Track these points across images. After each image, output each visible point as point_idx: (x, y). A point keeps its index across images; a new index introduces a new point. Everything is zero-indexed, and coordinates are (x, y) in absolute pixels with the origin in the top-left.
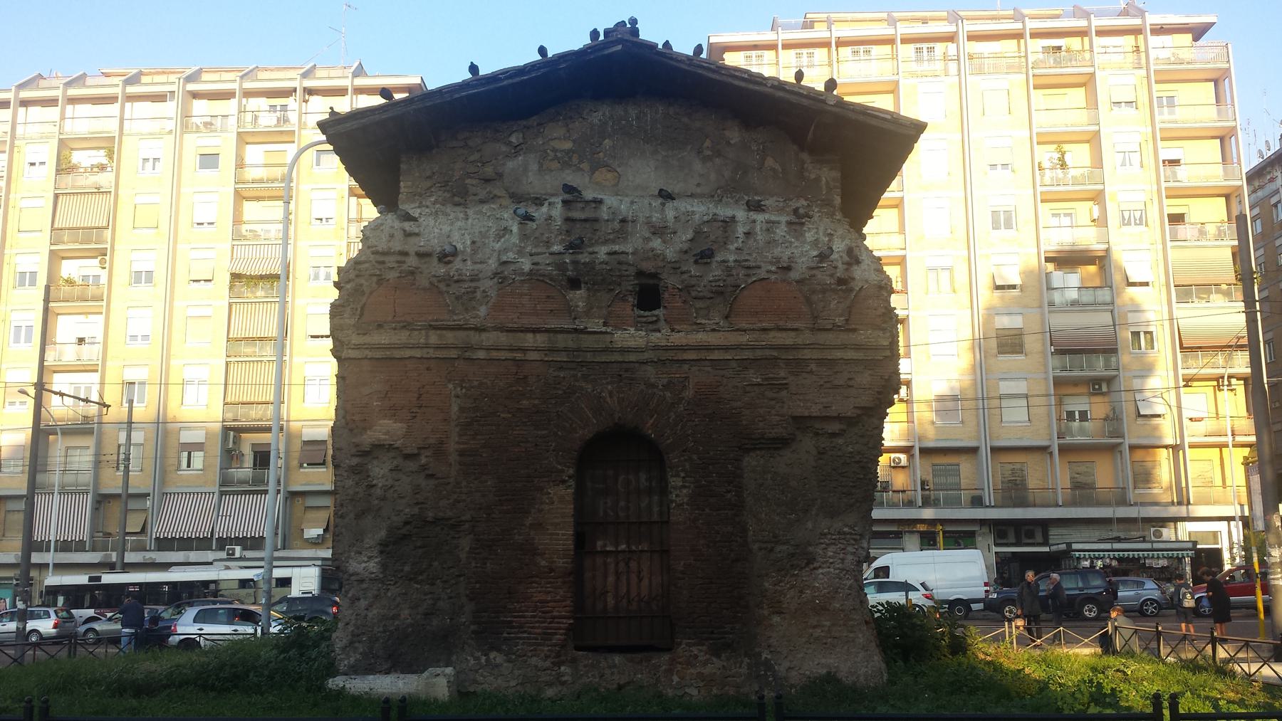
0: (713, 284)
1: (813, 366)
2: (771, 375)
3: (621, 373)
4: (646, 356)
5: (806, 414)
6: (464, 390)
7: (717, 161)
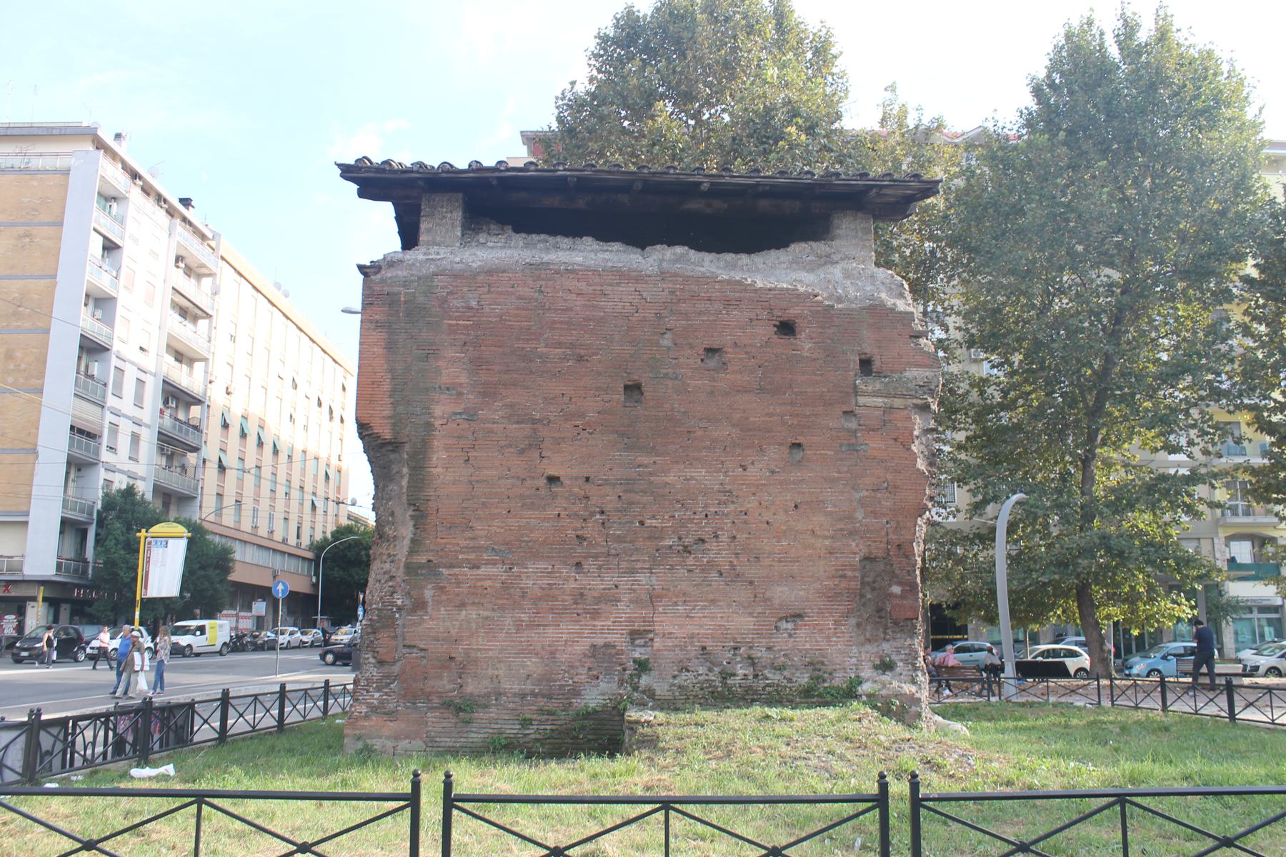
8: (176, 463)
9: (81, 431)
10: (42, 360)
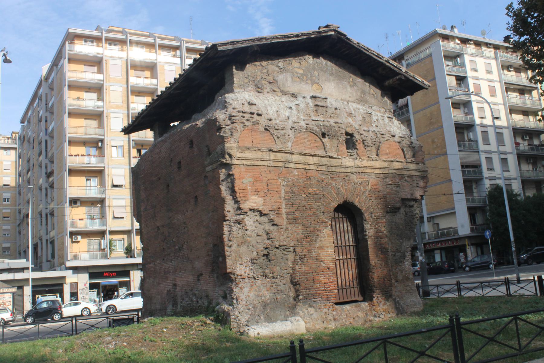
0: (373, 140)
1: (406, 178)
2: (394, 181)
3: (345, 177)
4: (353, 170)
5: (406, 198)
6: (286, 183)
7: (355, 88)
8: (539, 165)
9: (467, 166)
10: (444, 140)
